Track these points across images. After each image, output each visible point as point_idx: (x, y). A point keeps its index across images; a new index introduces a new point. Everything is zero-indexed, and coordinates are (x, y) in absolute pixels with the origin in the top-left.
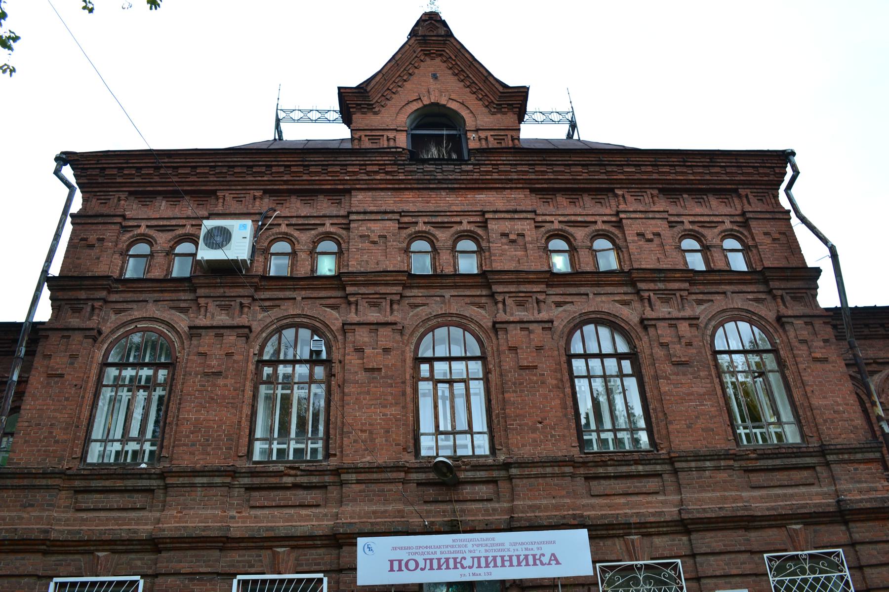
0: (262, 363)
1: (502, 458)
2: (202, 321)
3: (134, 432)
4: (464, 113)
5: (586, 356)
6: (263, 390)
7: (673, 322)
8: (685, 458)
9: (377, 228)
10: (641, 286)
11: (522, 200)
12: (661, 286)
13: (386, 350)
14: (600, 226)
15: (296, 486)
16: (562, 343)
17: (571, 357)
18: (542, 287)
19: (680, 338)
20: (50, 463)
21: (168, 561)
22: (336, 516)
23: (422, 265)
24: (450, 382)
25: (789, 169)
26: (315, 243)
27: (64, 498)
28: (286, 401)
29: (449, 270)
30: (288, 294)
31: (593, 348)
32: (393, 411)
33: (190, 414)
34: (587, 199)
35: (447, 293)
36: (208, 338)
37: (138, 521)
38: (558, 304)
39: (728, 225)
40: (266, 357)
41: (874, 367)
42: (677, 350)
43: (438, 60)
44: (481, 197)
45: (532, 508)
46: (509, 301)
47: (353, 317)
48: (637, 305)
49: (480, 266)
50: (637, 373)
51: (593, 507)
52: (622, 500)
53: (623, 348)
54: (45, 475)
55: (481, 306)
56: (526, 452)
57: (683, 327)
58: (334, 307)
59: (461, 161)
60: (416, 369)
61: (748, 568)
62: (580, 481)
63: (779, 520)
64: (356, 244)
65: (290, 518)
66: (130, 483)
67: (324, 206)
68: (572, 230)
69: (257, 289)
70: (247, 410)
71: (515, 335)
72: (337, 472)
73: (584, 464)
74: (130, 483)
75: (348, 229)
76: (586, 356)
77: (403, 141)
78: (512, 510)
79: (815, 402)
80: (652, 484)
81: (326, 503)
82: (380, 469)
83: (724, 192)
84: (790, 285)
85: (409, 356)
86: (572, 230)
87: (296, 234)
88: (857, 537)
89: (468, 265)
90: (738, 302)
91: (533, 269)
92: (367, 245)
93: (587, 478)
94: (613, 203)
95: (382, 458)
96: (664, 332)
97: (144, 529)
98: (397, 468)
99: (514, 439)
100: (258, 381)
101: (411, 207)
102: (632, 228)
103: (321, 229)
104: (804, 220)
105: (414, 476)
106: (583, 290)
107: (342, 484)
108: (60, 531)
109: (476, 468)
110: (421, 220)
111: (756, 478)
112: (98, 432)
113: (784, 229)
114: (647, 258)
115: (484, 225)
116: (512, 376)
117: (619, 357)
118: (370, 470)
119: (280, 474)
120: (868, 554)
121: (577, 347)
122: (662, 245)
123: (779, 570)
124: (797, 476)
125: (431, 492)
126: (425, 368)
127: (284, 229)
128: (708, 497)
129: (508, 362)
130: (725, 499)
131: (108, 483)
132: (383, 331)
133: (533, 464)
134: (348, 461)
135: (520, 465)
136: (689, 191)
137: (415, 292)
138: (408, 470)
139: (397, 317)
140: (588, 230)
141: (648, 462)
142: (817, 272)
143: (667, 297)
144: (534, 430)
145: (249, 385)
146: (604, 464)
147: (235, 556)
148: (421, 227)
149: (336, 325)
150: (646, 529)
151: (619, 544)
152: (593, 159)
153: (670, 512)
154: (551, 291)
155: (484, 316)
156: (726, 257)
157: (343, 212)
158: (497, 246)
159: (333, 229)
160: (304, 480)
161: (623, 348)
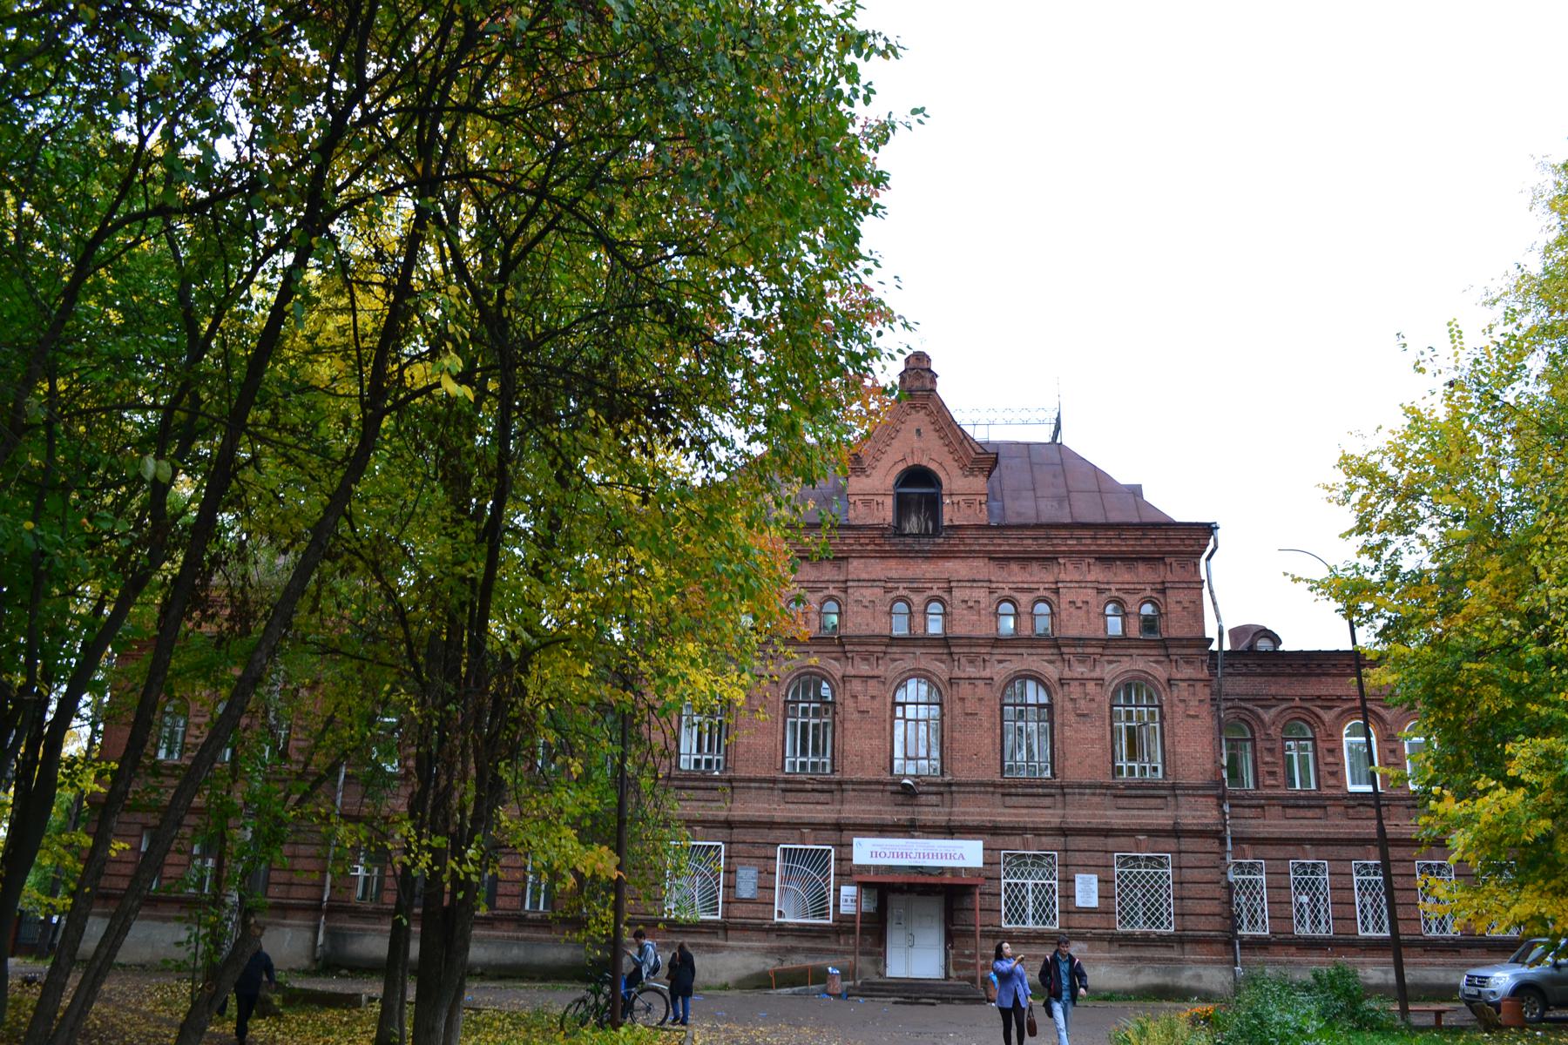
1: (948, 778)
4: (942, 475)
7: (1082, 681)
9: (866, 592)
10: (1064, 650)
11: (981, 568)
12: (1080, 650)
14: (1042, 593)
15: (813, 790)
17: (1003, 705)
18: (988, 650)
19: (1086, 694)
21: (738, 834)
23: (900, 628)
24: (917, 721)
25: (1212, 541)
26: (822, 604)
28: (805, 726)
29: (920, 632)
32: (876, 742)
34: (1035, 567)
35: (918, 651)
38: (1000, 662)
39: (1148, 593)
41: (1274, 702)
43: (922, 413)
44: (950, 565)
45: (964, 813)
46: (963, 660)
47: (850, 671)
48: (1059, 664)
49: (944, 628)
51: (1004, 815)
52: (1024, 811)
55: (942, 661)
56: (963, 777)
57: (1091, 686)
58: (836, 659)
60: (893, 711)
61: (1101, 862)
63: (1130, 832)
64: (852, 608)
65: (811, 811)
67: (829, 572)
68: (1018, 596)
70: (780, 737)
71: (965, 689)
72: (840, 783)
73: (1002, 786)
75: (845, 590)
77: (886, 513)
78: (950, 814)
79: (1179, 750)
80: (1047, 801)
81: (833, 802)
82: (868, 783)
83: (1152, 559)
84: (1185, 651)
86: (1018, 596)
88: (1183, 848)
89: (935, 628)
92: (860, 609)
93: (1003, 795)
94: (1056, 570)
95: (866, 777)
97: (722, 815)
98: (878, 783)
99: (957, 765)
101: (894, 575)
102: (1067, 595)
103: (826, 592)
104: (1211, 592)
109: (929, 784)
110: (901, 585)
111: (1121, 802)
113: (1195, 598)
114: (1074, 627)
115: (950, 590)
116: (960, 719)
117: (1040, 706)
118: (860, 783)
119: (803, 782)
120: (1187, 859)
122: (1088, 612)
123: (1123, 865)
124: (1152, 802)
125: (900, 798)
126: (899, 710)
128: (1080, 815)
129: (958, 708)
130: (1094, 816)
131: (696, 784)
132: (872, 683)
133: (966, 784)
134: (846, 777)
135: (959, 784)
136: (1121, 559)
137: (894, 649)
138: (885, 784)
139: (880, 671)
140: (1032, 596)
141: (1047, 787)
142: (1211, 640)
143: (1083, 659)
144: (971, 760)
145: (780, 719)
147: (778, 833)
149: (838, 676)
150: (1037, 831)
151: (1018, 839)
152: (1041, 533)
155: (941, 669)
157: (842, 578)
158: (959, 611)
159: (834, 593)
160: (819, 787)
161: (1044, 699)
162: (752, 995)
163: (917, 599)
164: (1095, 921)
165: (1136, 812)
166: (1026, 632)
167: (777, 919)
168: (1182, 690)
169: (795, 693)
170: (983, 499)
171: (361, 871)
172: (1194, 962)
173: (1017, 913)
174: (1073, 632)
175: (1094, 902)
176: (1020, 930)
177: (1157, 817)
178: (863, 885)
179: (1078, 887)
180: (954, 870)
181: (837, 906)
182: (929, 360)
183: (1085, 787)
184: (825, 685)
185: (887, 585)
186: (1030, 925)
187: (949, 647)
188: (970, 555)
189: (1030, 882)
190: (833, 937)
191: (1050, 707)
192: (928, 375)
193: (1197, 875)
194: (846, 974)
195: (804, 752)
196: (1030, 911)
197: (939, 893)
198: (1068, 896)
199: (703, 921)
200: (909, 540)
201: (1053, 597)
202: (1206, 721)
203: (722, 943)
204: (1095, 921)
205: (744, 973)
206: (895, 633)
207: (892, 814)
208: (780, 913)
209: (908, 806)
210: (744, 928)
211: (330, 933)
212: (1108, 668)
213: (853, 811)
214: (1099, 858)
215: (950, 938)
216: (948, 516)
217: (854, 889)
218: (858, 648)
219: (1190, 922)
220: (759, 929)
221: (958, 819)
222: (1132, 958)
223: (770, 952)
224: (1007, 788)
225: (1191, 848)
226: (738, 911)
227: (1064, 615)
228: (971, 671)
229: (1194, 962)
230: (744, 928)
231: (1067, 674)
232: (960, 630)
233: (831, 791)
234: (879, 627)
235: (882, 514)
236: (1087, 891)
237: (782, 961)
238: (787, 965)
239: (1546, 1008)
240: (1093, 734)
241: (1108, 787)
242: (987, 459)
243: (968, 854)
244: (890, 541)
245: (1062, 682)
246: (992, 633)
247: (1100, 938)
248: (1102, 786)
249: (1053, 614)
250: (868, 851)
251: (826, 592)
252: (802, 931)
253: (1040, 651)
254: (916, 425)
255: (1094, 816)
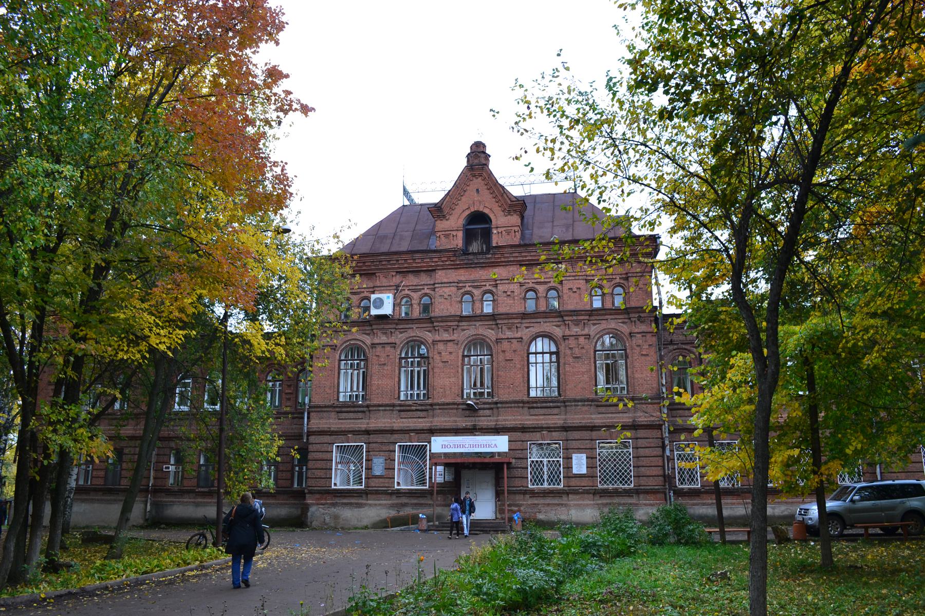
0: (401, 358)
2: (376, 341)
3: (355, 389)
4: (492, 216)
5: (536, 353)
6: (403, 369)
7: (577, 337)
8: (568, 401)
9: (447, 290)
10: (566, 318)
12: (575, 318)
13: (450, 353)
15: (417, 410)
16: (526, 348)
17: (529, 354)
20: (328, 403)
21: (373, 438)
22: (431, 422)
23: (467, 311)
26: (421, 299)
27: (333, 415)
29: (478, 312)
30: (410, 326)
31: (540, 350)
32: (453, 380)
33: (375, 381)
35: (478, 324)
36: (379, 348)
37: (361, 423)
38: (527, 327)
39: (618, 280)
40: (403, 355)
42: (577, 351)
43: (480, 179)
44: (496, 270)
45: (505, 420)
46: (504, 327)
47: (437, 338)
49: (493, 309)
50: (558, 361)
52: (542, 417)
53: (554, 349)
54: (326, 407)
55: (492, 329)
57: (582, 339)
58: (429, 331)
59: (488, 252)
60: (463, 360)
62: (526, 409)
64: (438, 300)
66: (356, 409)
67: (424, 279)
68: (537, 287)
69: (397, 324)
70: (397, 379)
71: (505, 345)
72: (431, 405)
73: (528, 402)
74: (356, 409)
76: (536, 353)
77: (458, 241)
78: (497, 421)
79: (637, 376)
80: (556, 411)
82: (448, 404)
85: (461, 354)
86: (537, 287)
87: (412, 294)
88: (639, 436)
89: (488, 309)
90: (613, 325)
91: (516, 311)
92: (443, 300)
93: (529, 408)
96: (572, 342)
98: (454, 404)
99: (501, 392)
100: (400, 367)
101: (463, 278)
103: (423, 291)
105: (461, 407)
106: (539, 320)
107: (434, 409)
108: (334, 427)
112: (341, 389)
114: (572, 304)
115: (496, 286)
117: (551, 353)
118: (444, 404)
119: (410, 406)
121: (532, 349)
126: (466, 359)
127: (407, 292)
128: (577, 417)
130: (584, 418)
132: (450, 344)
133: (506, 403)
135: (501, 403)
137: (464, 323)
138: (459, 404)
139: (455, 337)
144: (509, 388)
146: (536, 402)
147: (396, 436)
148: (468, 289)
149: (430, 341)
150: (550, 429)
151: (538, 434)
153: (560, 422)
154: (524, 321)
156: (613, 299)
158: (502, 298)
159: (428, 291)
160: (420, 408)
161: (554, 349)
162: (379, 531)
163: (477, 292)
164: (585, 482)
165: (610, 415)
166: (543, 308)
167: (396, 487)
168: (638, 339)
169: (407, 353)
170: (516, 229)
171: (172, 468)
172: (645, 505)
173: (538, 479)
174: (571, 307)
175: (584, 471)
176: (539, 489)
177: (623, 418)
178: (447, 465)
179: (574, 461)
180: (492, 454)
181: (430, 478)
182: (484, 146)
183: (578, 401)
184: (423, 347)
185: (459, 285)
186: (546, 485)
187: (495, 320)
188: (507, 264)
189: (545, 460)
190: (429, 496)
191: (557, 353)
192: (483, 155)
193: (647, 452)
194: (429, 519)
195: (412, 388)
196: (545, 477)
197: (491, 468)
198: (569, 467)
199: (353, 490)
200: (471, 257)
201: (560, 287)
202: (653, 356)
203: (364, 502)
204: (585, 482)
205: (378, 519)
206: (464, 314)
207: (463, 423)
208: (398, 484)
209: (471, 417)
210: (377, 492)
211: (155, 504)
212: (593, 328)
213: (440, 421)
214: (588, 444)
215: (498, 494)
216: (496, 240)
217: (442, 467)
218: (442, 324)
219: (643, 481)
220: (385, 493)
221: (501, 423)
222: (607, 504)
223: (392, 506)
224: (532, 404)
225: (645, 436)
226: (373, 483)
227: (565, 297)
228: (509, 334)
229: (645, 505)
230: (377, 492)
231: (567, 333)
232: (502, 310)
233: (426, 410)
234: (453, 310)
235: (455, 243)
236: (579, 464)
237: (399, 512)
238: (401, 513)
239: (844, 527)
240: (583, 369)
241: (592, 401)
242: (520, 206)
243: (500, 444)
244: (461, 258)
245: (565, 338)
246: (522, 310)
247: (587, 492)
248: (588, 400)
249: (559, 296)
250: (440, 445)
251: (423, 291)
252: (411, 494)
253: (551, 320)
254: (476, 186)
255: (584, 418)
